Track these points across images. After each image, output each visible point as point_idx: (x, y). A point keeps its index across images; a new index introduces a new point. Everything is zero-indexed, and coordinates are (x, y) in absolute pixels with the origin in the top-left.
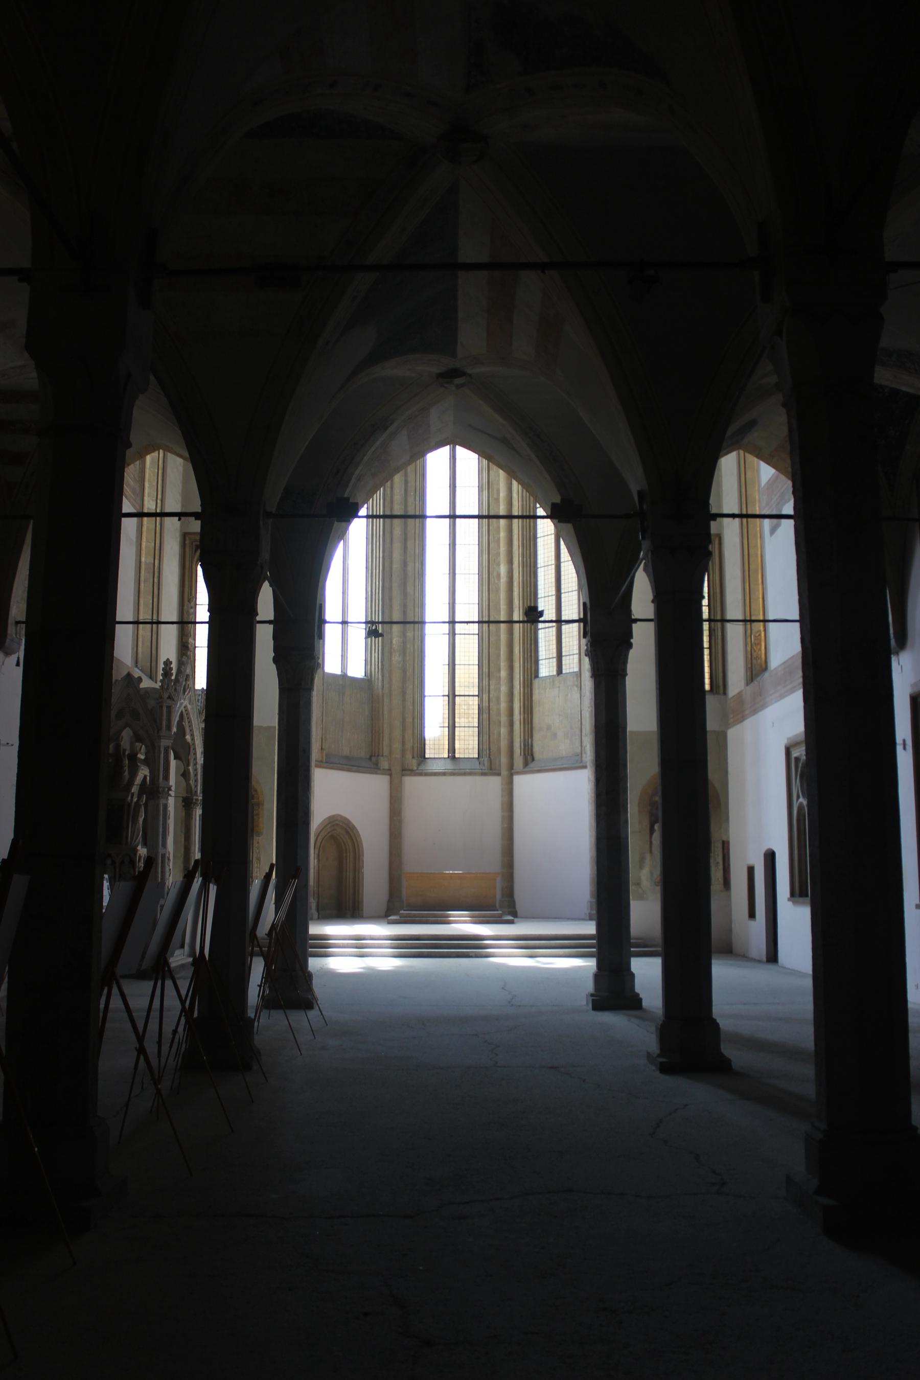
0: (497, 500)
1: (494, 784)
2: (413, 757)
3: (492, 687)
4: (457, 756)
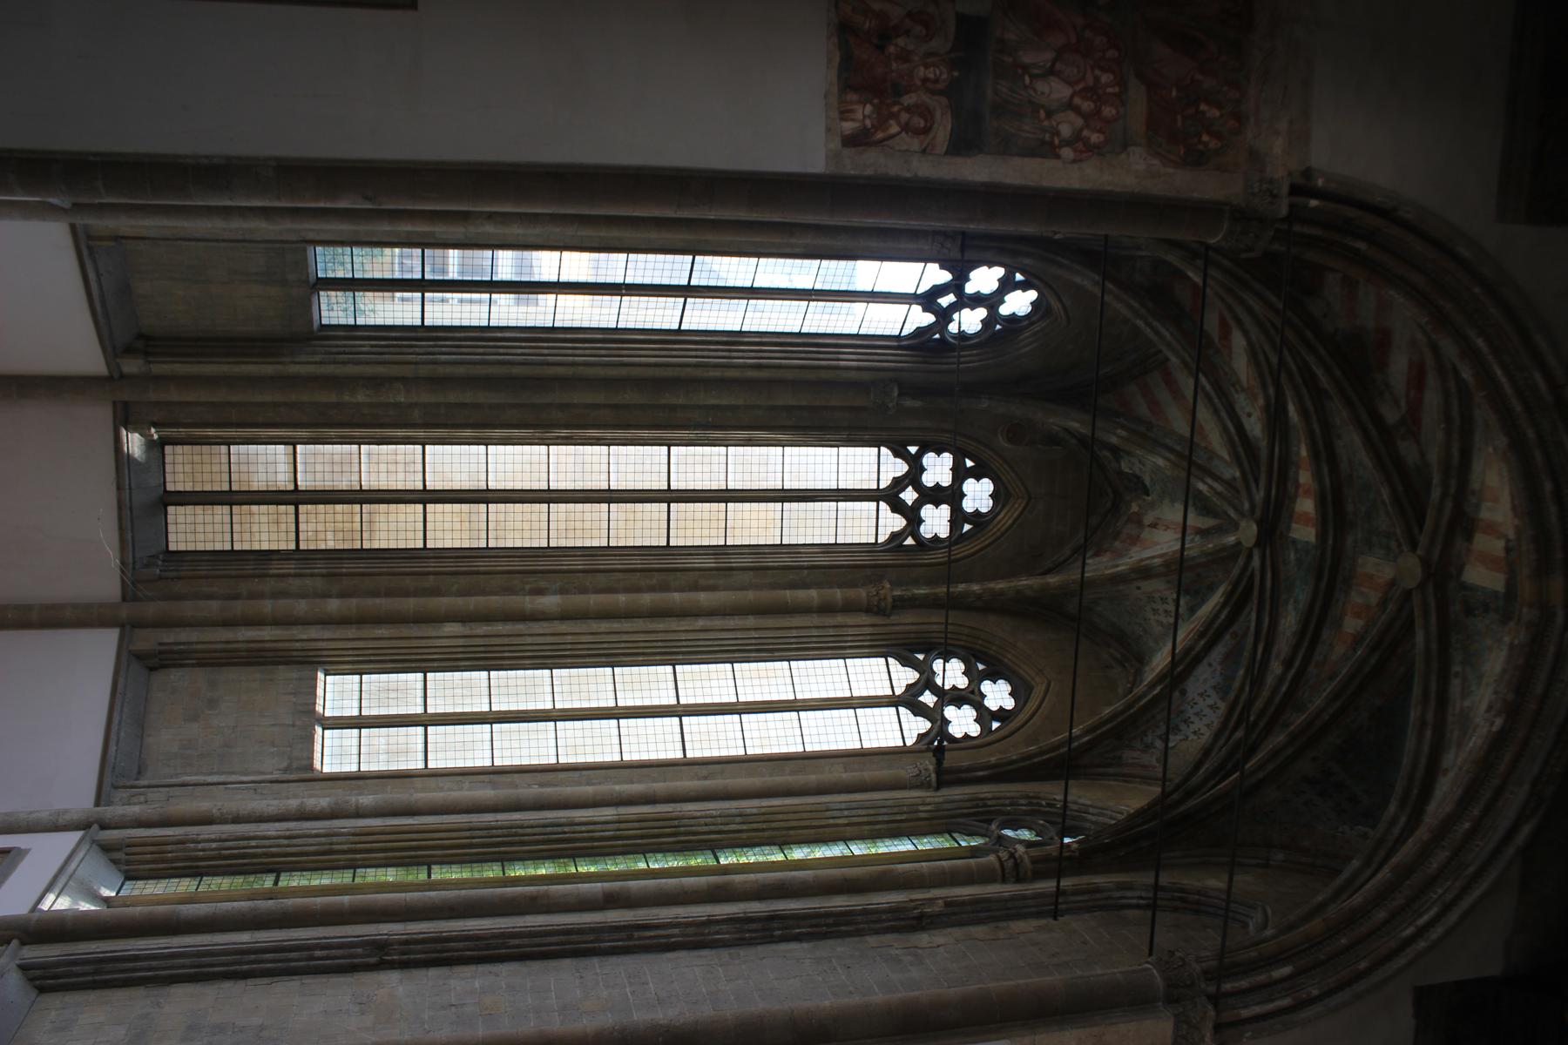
0: (696, 587)
1: (105, 584)
3: (308, 581)
4: (171, 509)
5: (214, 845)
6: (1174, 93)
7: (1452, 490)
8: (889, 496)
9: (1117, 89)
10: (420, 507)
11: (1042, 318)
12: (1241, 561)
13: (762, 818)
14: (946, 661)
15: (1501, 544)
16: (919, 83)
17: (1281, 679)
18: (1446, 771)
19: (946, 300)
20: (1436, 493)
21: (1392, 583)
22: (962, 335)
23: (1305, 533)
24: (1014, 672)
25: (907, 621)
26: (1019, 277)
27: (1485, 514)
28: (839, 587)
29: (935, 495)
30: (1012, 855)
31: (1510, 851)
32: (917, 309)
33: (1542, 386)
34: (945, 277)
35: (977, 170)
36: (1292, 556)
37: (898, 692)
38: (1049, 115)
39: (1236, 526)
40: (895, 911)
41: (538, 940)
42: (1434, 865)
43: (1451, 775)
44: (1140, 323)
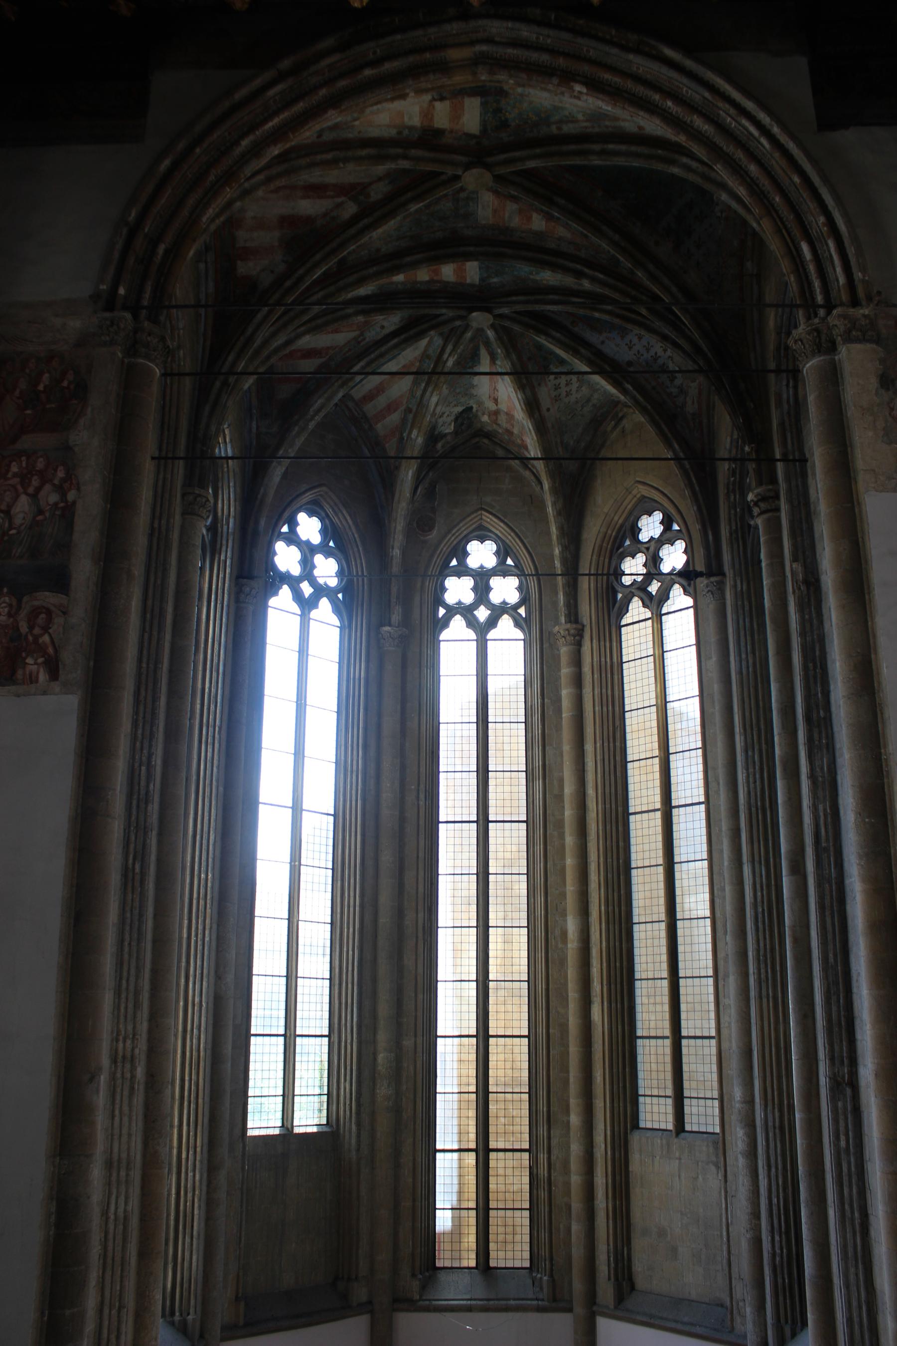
0: (560, 797)
2: (414, 1275)
3: (554, 1142)
4: (492, 1264)
5: (777, 1238)
6: (29, 412)
7: (400, 151)
8: (482, 631)
9: (23, 458)
10: (492, 1041)
11: (322, 508)
12: (507, 324)
13: (749, 731)
14: (623, 574)
15: (438, 105)
16: (11, 620)
17: (593, 279)
18: (640, 128)
19: (307, 589)
20: (404, 164)
21: (496, 193)
22: (340, 574)
23: (472, 271)
24: (630, 513)
25: (587, 610)
26: (285, 529)
27: (416, 121)
28: (559, 670)
29: (482, 590)
30: (756, 504)
31: (689, 63)
32: (314, 614)
33: (280, 87)
34: (285, 592)
35: (83, 570)
36: (495, 280)
37: (649, 615)
38: (41, 512)
39: (480, 331)
40: (802, 607)
41: (830, 937)
42: (706, 128)
43: (642, 123)
44: (312, 425)
